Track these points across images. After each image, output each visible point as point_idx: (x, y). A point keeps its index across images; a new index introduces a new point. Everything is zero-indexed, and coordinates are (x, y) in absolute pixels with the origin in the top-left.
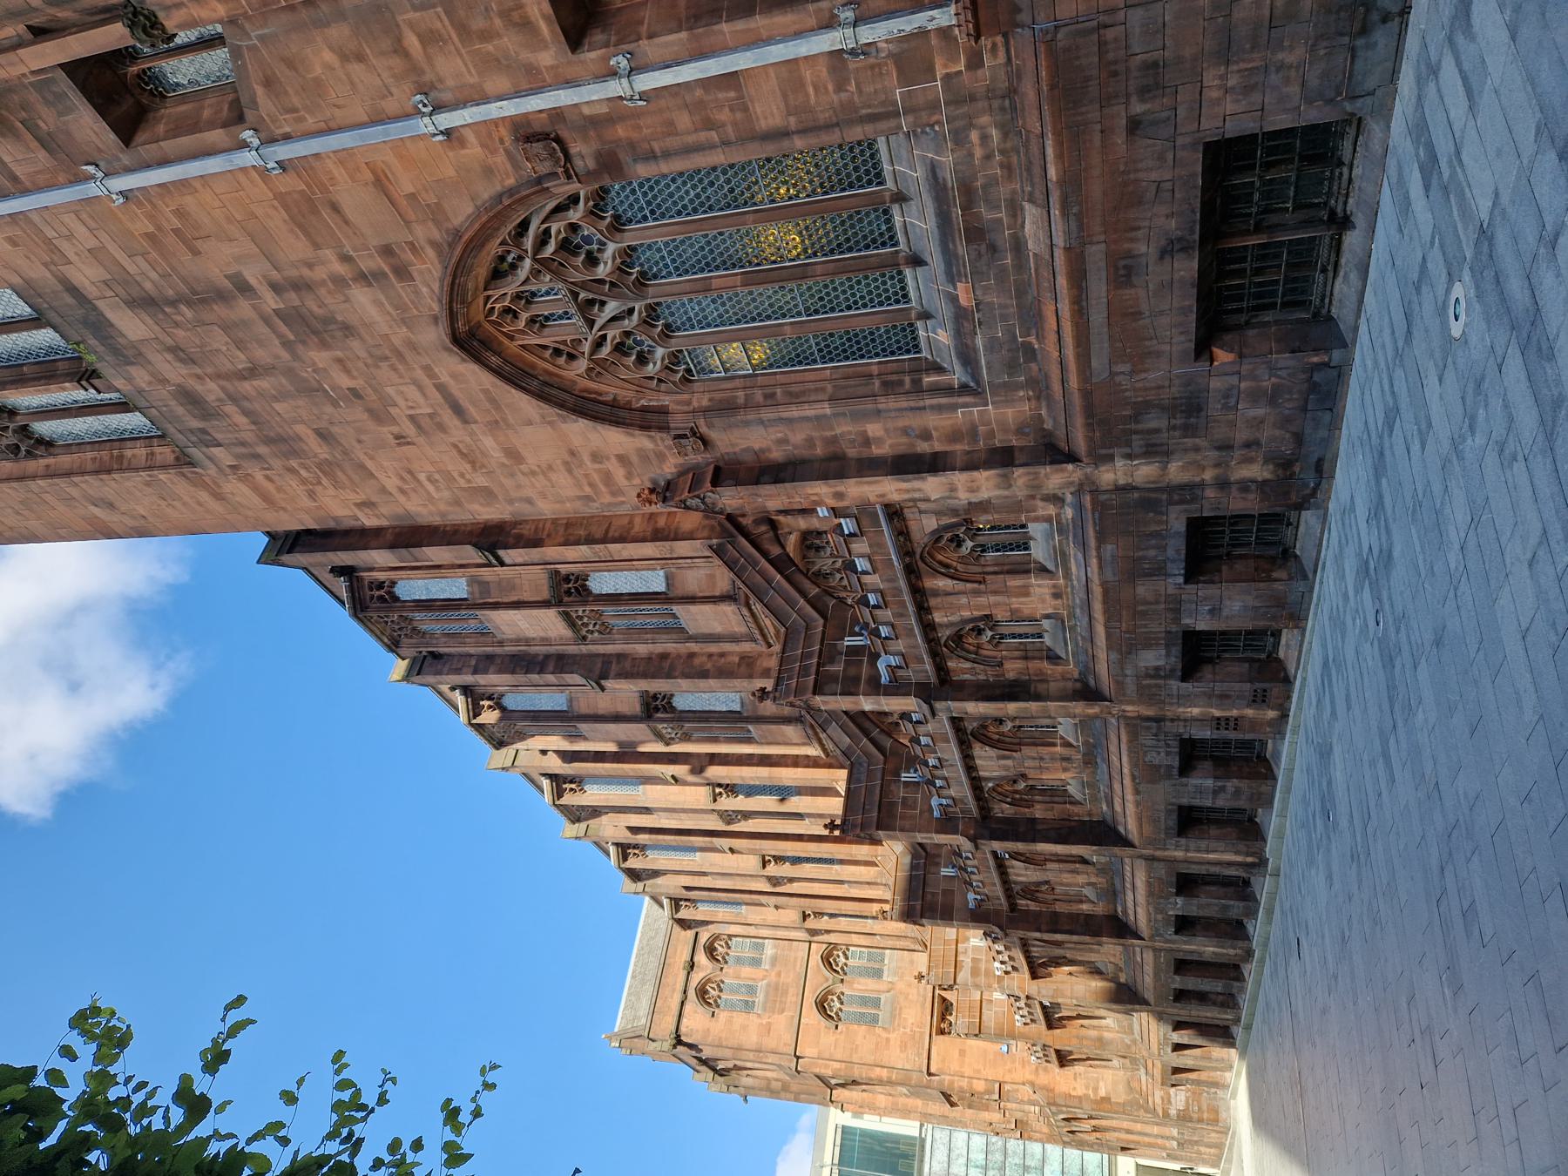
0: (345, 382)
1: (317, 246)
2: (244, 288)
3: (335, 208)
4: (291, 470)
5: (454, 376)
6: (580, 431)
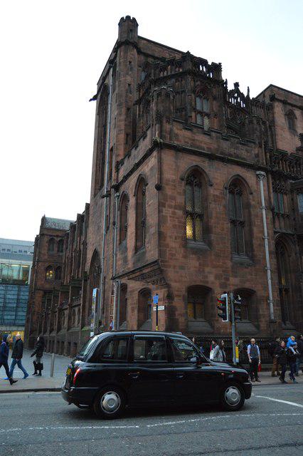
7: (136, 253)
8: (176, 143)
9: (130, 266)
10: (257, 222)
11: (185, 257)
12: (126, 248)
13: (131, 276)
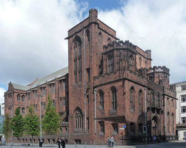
2: (81, 97)
6: (73, 111)
8: (128, 78)
9: (107, 115)
10: (144, 103)
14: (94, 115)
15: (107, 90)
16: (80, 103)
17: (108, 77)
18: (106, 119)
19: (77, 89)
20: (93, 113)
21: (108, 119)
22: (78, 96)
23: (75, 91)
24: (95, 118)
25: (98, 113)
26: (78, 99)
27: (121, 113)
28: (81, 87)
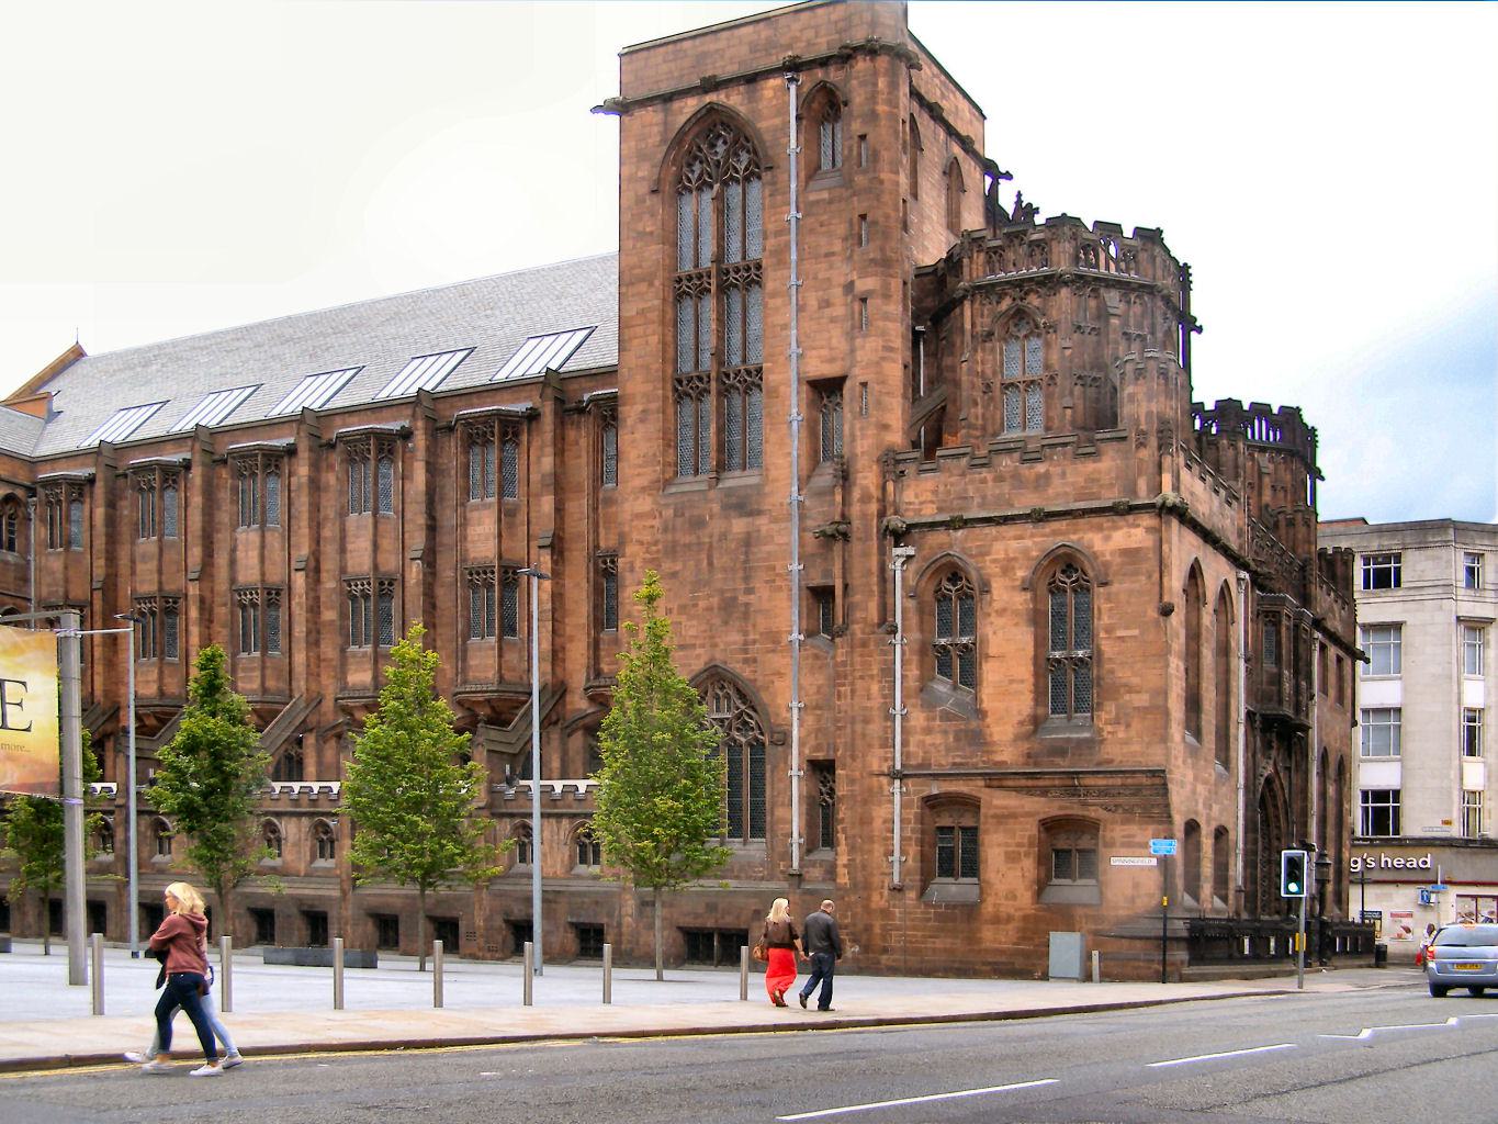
0: (702, 604)
1: (761, 634)
2: (749, 591)
3: (773, 651)
4: (656, 543)
5: (698, 656)
7: (1035, 731)
11: (1184, 762)
12: (981, 714)
13: (1010, 783)
14: (888, 743)
15: (1007, 568)
16: (735, 637)
17: (1016, 476)
18: (997, 779)
19: (716, 526)
20: (875, 729)
21: (1023, 782)
22: (718, 585)
23: (687, 539)
24: (898, 767)
25: (928, 731)
26: (715, 601)
27: (1136, 748)
28: (759, 513)
